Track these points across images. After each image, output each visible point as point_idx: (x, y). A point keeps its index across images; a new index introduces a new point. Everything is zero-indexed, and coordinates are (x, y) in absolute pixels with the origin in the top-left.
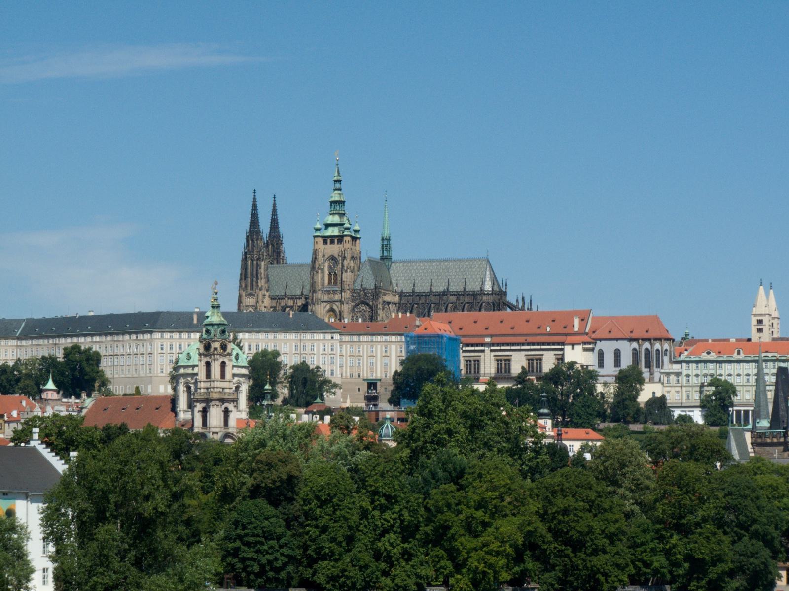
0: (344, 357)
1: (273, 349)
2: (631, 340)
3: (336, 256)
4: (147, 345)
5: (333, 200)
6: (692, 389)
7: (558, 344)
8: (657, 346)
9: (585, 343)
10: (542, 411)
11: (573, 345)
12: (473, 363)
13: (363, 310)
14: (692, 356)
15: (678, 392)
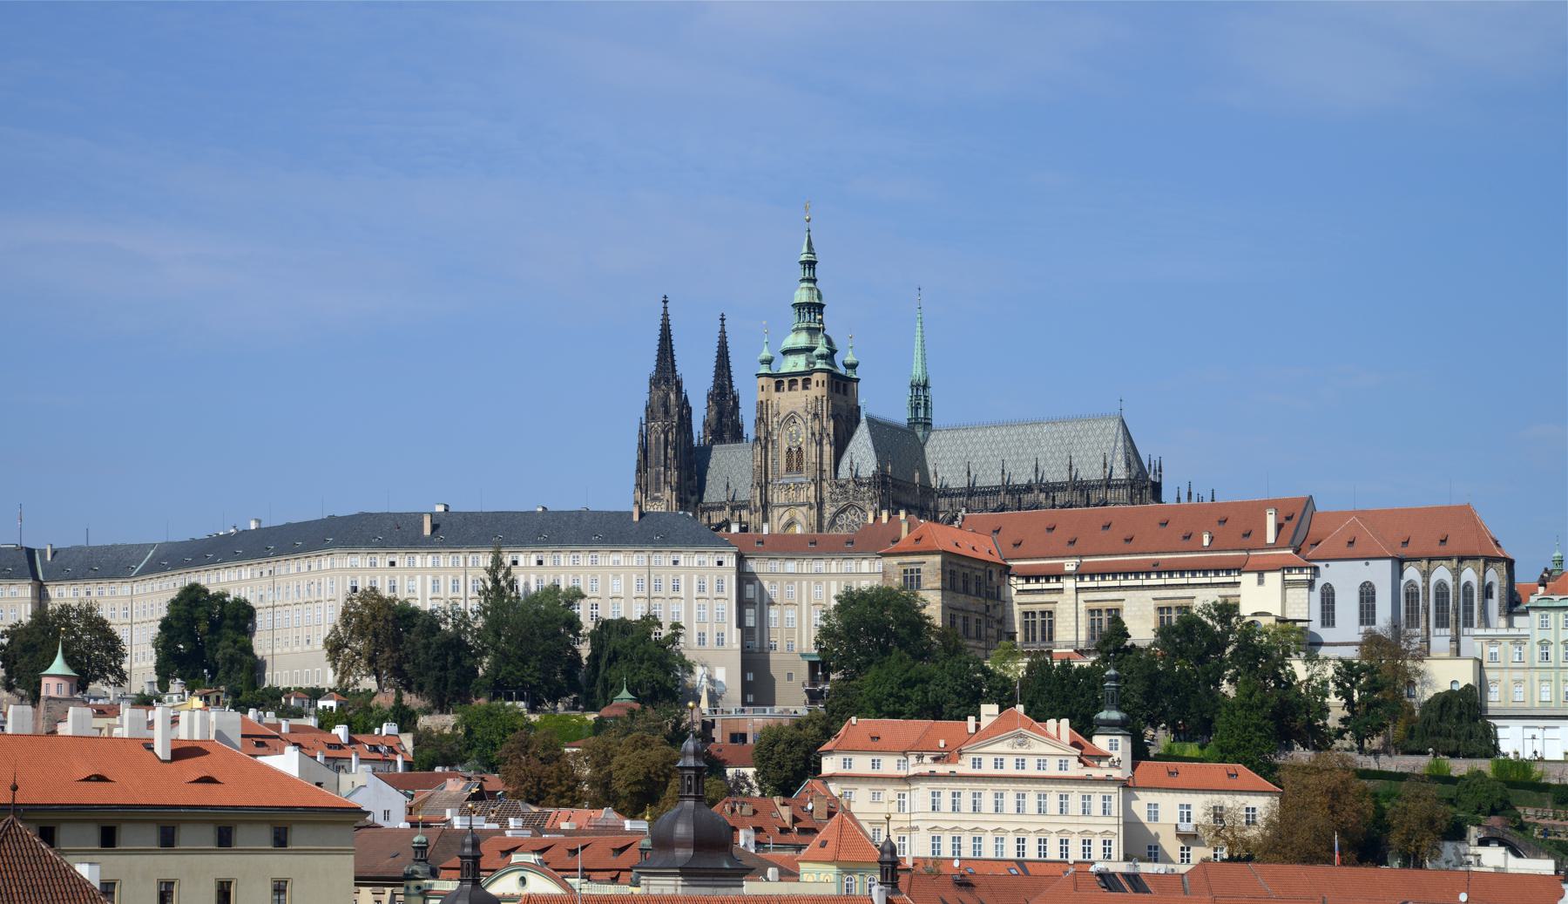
0: (757, 607)
1: (571, 584)
2: (1400, 563)
3: (801, 412)
4: (325, 581)
5: (797, 300)
6: (1557, 674)
7: (1228, 572)
8: (1469, 574)
9: (1290, 569)
10: (1103, 715)
11: (1261, 573)
12: (1038, 618)
13: (853, 521)
14: (1556, 598)
15: (1518, 682)
